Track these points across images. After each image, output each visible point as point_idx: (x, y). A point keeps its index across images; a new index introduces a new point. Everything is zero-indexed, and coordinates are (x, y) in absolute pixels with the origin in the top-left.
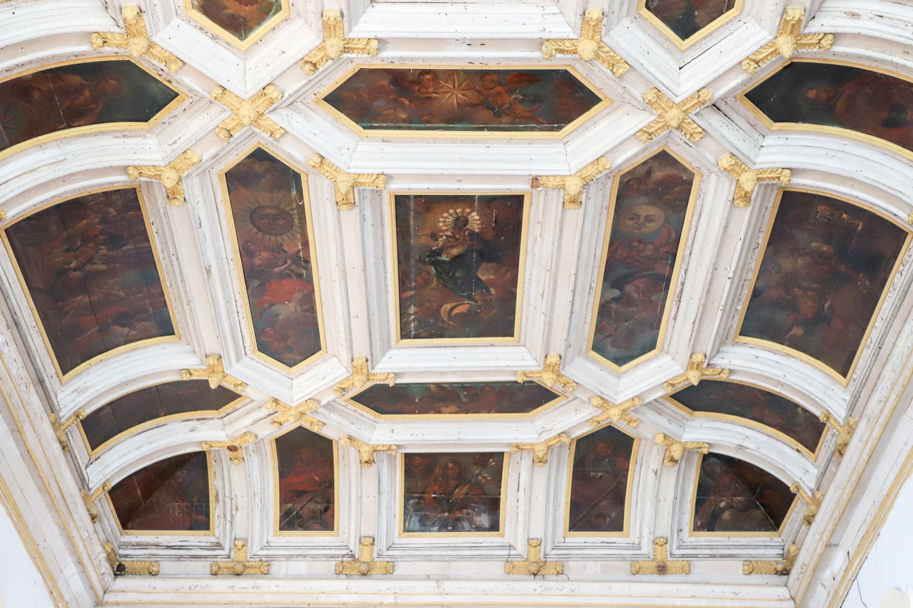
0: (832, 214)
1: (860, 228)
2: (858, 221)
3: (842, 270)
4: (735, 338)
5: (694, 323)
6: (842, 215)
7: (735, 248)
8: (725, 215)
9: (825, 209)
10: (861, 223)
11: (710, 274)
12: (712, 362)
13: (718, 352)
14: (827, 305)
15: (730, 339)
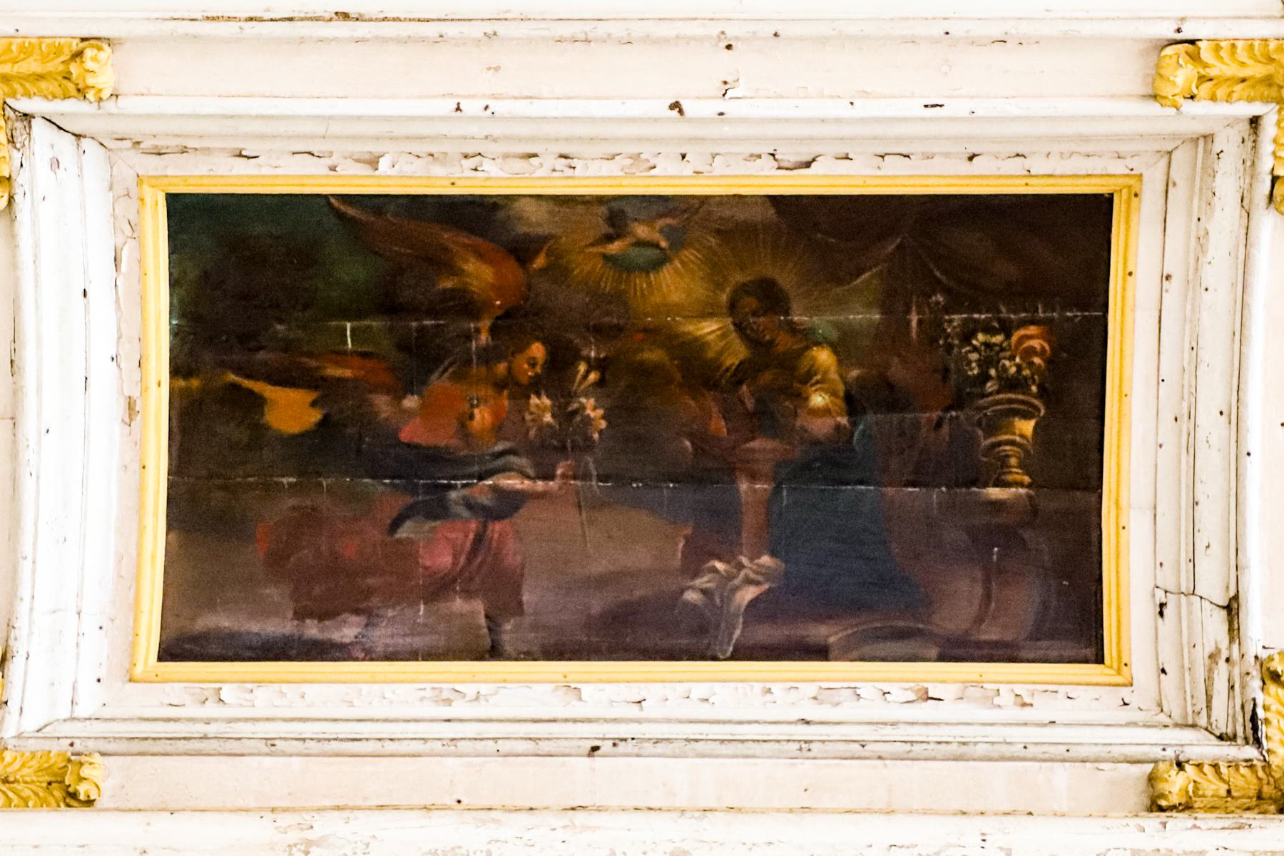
0: (1013, 384)
1: (994, 493)
2: (1027, 479)
3: (744, 486)
4: (155, 180)
5: (346, 16)
6: (1026, 416)
7: (865, 94)
8: (1087, 29)
9: (1031, 352)
10: (1022, 491)
11: (714, 30)
12: (37, 124)
13: (78, 136)
14: (512, 482)
15: (152, 165)
